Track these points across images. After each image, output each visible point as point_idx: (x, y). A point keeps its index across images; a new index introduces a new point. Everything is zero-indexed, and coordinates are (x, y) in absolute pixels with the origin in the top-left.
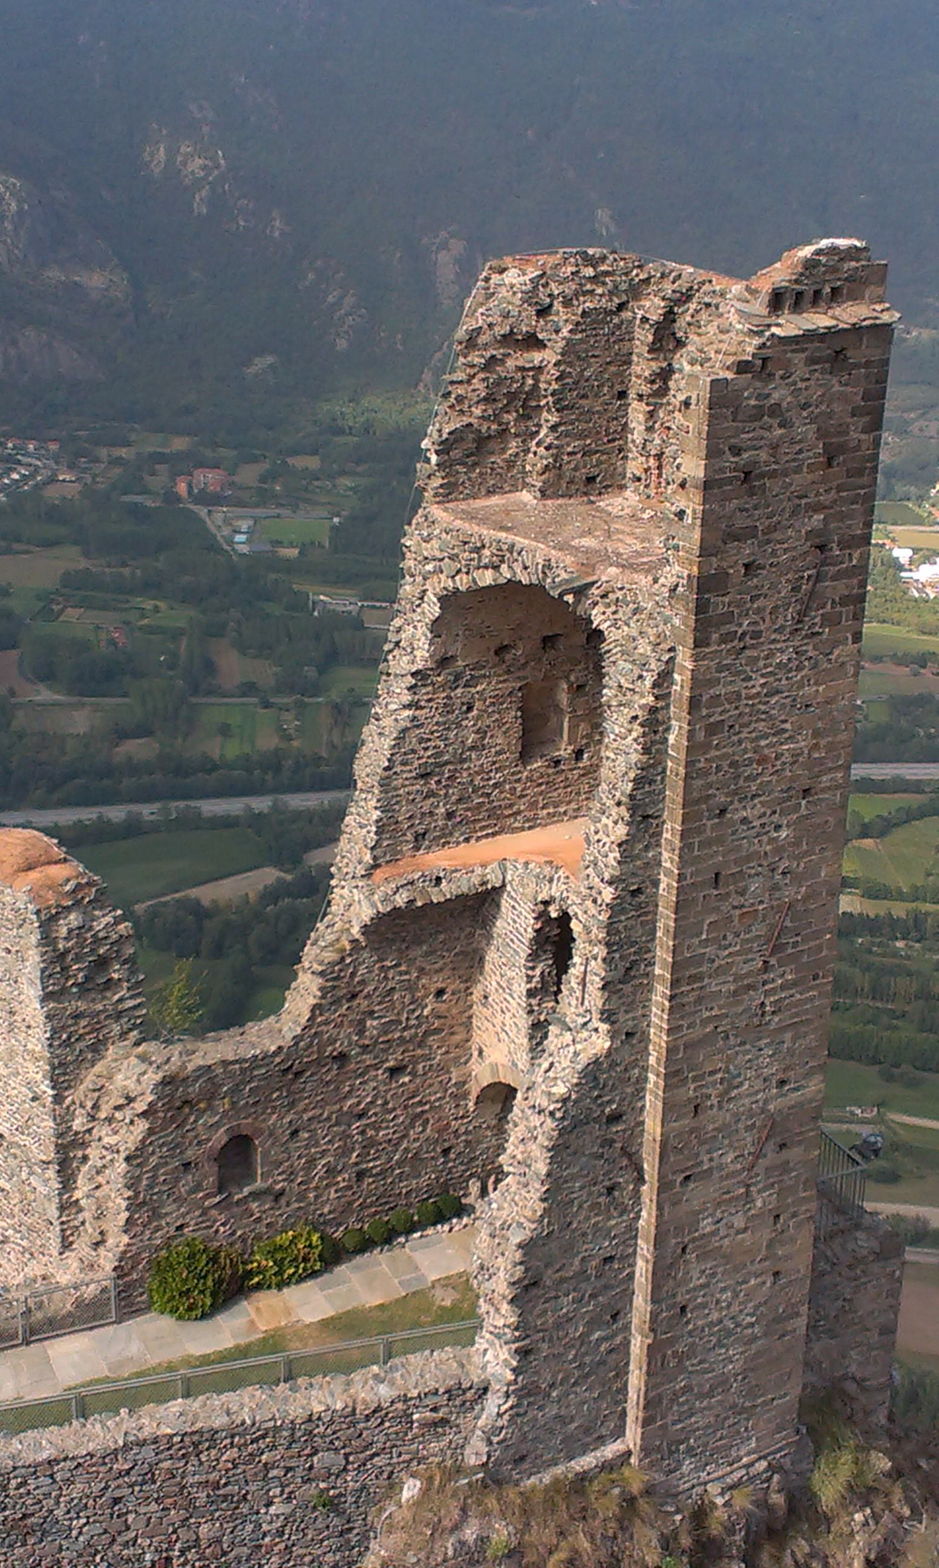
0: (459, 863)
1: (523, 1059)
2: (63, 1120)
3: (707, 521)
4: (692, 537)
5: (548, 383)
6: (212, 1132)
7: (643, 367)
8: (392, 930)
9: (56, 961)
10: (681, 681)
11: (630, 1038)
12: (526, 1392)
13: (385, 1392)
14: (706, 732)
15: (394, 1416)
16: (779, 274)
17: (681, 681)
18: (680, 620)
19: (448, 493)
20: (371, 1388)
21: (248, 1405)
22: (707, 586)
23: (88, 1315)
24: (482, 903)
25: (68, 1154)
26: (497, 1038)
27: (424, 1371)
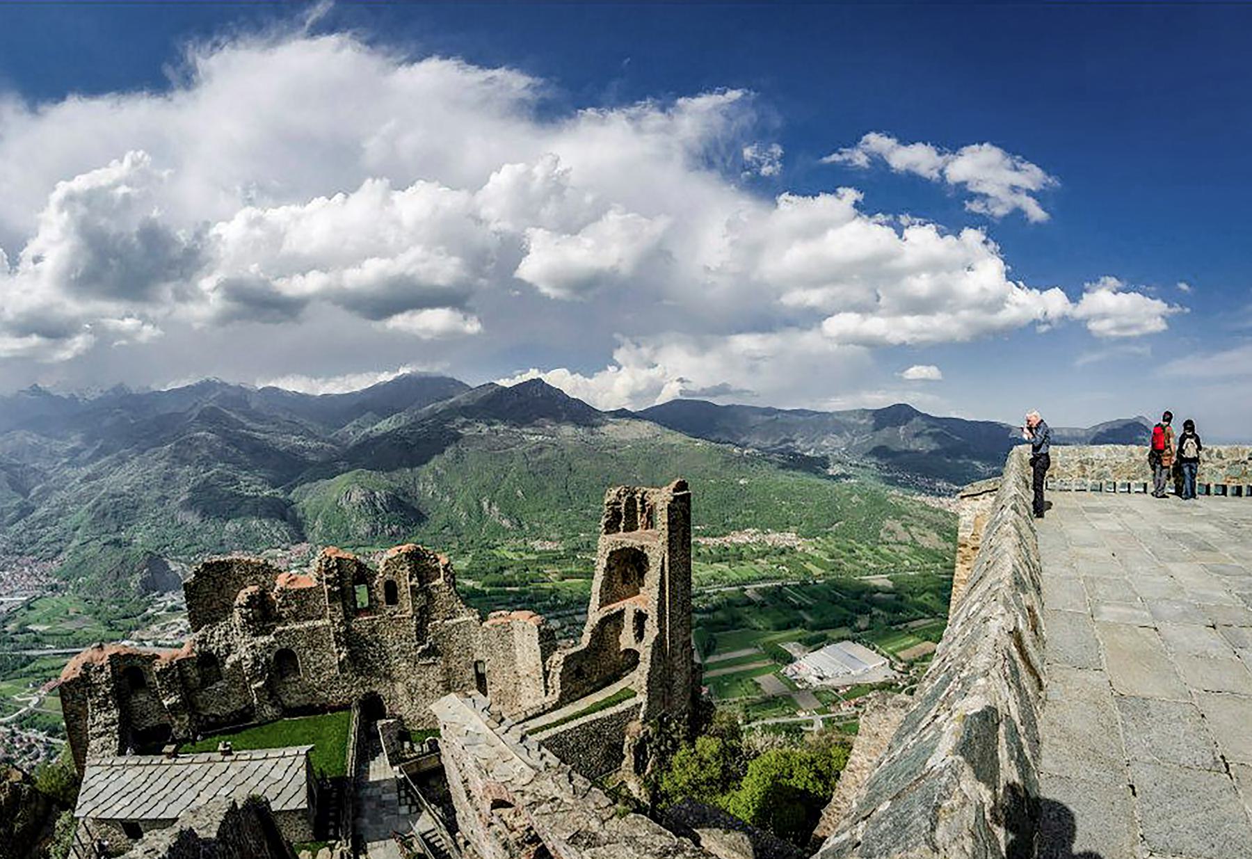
0: (616, 607)
1: (633, 642)
2: (544, 669)
3: (669, 530)
4: (667, 533)
5: (623, 511)
6: (574, 666)
7: (639, 506)
8: (603, 621)
9: (541, 634)
10: (666, 560)
11: (662, 631)
12: (649, 703)
13: (623, 708)
14: (671, 569)
15: (626, 712)
16: (673, 485)
17: (666, 560)
18: (666, 548)
19: (607, 533)
20: (620, 708)
21: (599, 715)
22: (670, 541)
23: (556, 707)
24: (621, 613)
25: (546, 674)
26: (627, 639)
27: (629, 703)
